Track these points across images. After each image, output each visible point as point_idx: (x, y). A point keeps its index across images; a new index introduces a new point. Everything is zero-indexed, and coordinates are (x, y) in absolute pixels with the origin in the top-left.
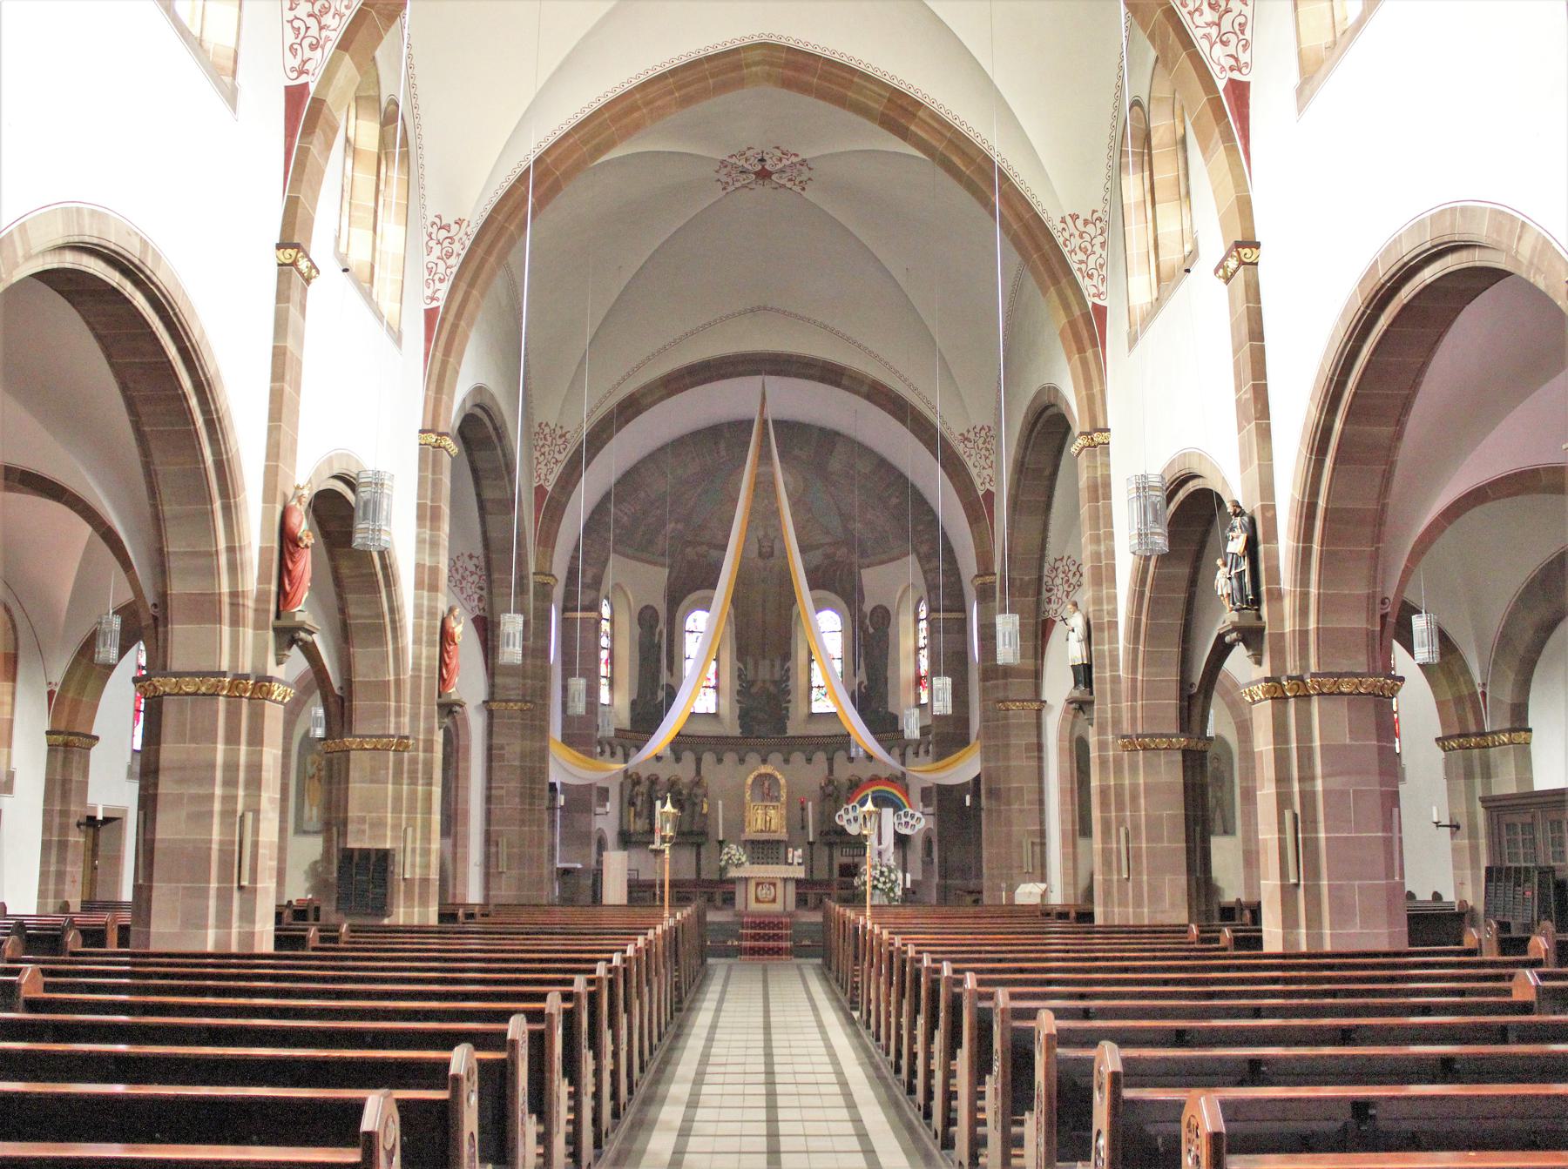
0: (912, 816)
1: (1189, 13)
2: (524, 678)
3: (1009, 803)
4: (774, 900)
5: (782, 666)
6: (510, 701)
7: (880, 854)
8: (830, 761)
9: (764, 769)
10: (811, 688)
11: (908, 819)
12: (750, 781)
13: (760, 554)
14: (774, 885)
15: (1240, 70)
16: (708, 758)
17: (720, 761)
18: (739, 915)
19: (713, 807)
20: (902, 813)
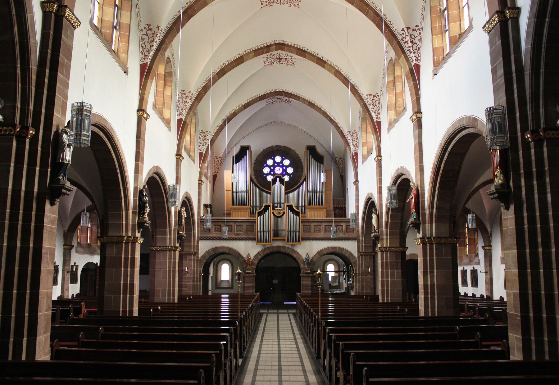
1: (405, 43)
15: (418, 61)
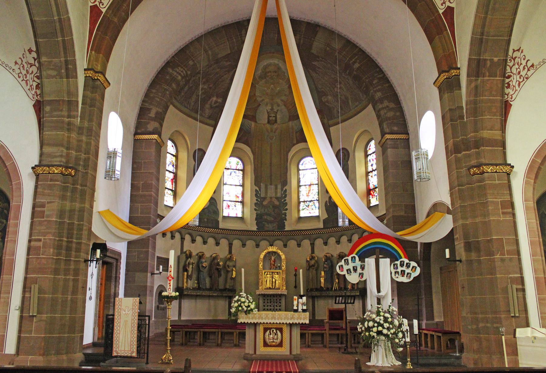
0: (408, 266)
2: (68, 148)
3: (490, 253)
4: (280, 345)
5: (282, 190)
6: (53, 166)
7: (379, 301)
8: (312, 245)
9: (271, 249)
10: (299, 203)
11: (404, 268)
12: (262, 256)
13: (269, 122)
14: (281, 330)
16: (237, 243)
17: (244, 245)
18: (246, 358)
19: (239, 273)
20: (398, 263)
